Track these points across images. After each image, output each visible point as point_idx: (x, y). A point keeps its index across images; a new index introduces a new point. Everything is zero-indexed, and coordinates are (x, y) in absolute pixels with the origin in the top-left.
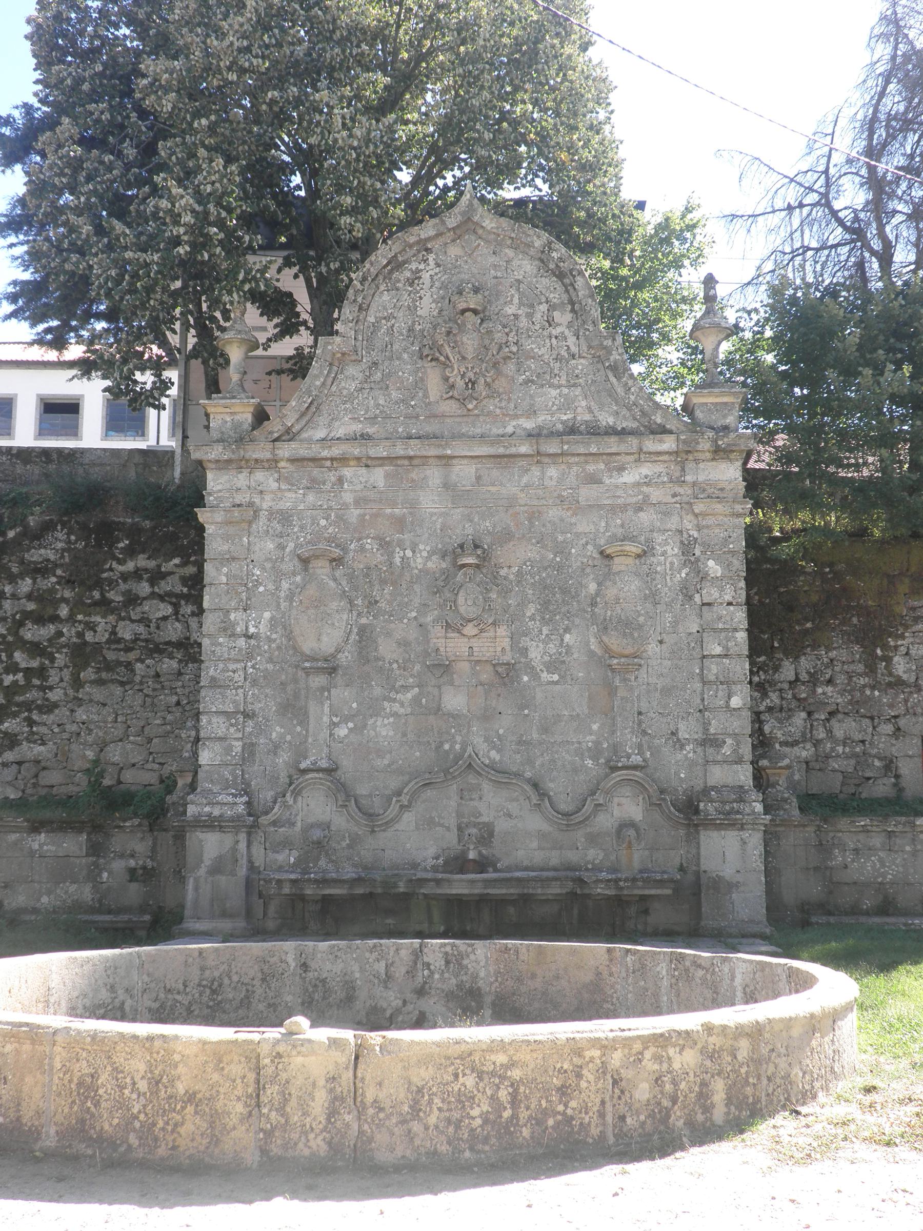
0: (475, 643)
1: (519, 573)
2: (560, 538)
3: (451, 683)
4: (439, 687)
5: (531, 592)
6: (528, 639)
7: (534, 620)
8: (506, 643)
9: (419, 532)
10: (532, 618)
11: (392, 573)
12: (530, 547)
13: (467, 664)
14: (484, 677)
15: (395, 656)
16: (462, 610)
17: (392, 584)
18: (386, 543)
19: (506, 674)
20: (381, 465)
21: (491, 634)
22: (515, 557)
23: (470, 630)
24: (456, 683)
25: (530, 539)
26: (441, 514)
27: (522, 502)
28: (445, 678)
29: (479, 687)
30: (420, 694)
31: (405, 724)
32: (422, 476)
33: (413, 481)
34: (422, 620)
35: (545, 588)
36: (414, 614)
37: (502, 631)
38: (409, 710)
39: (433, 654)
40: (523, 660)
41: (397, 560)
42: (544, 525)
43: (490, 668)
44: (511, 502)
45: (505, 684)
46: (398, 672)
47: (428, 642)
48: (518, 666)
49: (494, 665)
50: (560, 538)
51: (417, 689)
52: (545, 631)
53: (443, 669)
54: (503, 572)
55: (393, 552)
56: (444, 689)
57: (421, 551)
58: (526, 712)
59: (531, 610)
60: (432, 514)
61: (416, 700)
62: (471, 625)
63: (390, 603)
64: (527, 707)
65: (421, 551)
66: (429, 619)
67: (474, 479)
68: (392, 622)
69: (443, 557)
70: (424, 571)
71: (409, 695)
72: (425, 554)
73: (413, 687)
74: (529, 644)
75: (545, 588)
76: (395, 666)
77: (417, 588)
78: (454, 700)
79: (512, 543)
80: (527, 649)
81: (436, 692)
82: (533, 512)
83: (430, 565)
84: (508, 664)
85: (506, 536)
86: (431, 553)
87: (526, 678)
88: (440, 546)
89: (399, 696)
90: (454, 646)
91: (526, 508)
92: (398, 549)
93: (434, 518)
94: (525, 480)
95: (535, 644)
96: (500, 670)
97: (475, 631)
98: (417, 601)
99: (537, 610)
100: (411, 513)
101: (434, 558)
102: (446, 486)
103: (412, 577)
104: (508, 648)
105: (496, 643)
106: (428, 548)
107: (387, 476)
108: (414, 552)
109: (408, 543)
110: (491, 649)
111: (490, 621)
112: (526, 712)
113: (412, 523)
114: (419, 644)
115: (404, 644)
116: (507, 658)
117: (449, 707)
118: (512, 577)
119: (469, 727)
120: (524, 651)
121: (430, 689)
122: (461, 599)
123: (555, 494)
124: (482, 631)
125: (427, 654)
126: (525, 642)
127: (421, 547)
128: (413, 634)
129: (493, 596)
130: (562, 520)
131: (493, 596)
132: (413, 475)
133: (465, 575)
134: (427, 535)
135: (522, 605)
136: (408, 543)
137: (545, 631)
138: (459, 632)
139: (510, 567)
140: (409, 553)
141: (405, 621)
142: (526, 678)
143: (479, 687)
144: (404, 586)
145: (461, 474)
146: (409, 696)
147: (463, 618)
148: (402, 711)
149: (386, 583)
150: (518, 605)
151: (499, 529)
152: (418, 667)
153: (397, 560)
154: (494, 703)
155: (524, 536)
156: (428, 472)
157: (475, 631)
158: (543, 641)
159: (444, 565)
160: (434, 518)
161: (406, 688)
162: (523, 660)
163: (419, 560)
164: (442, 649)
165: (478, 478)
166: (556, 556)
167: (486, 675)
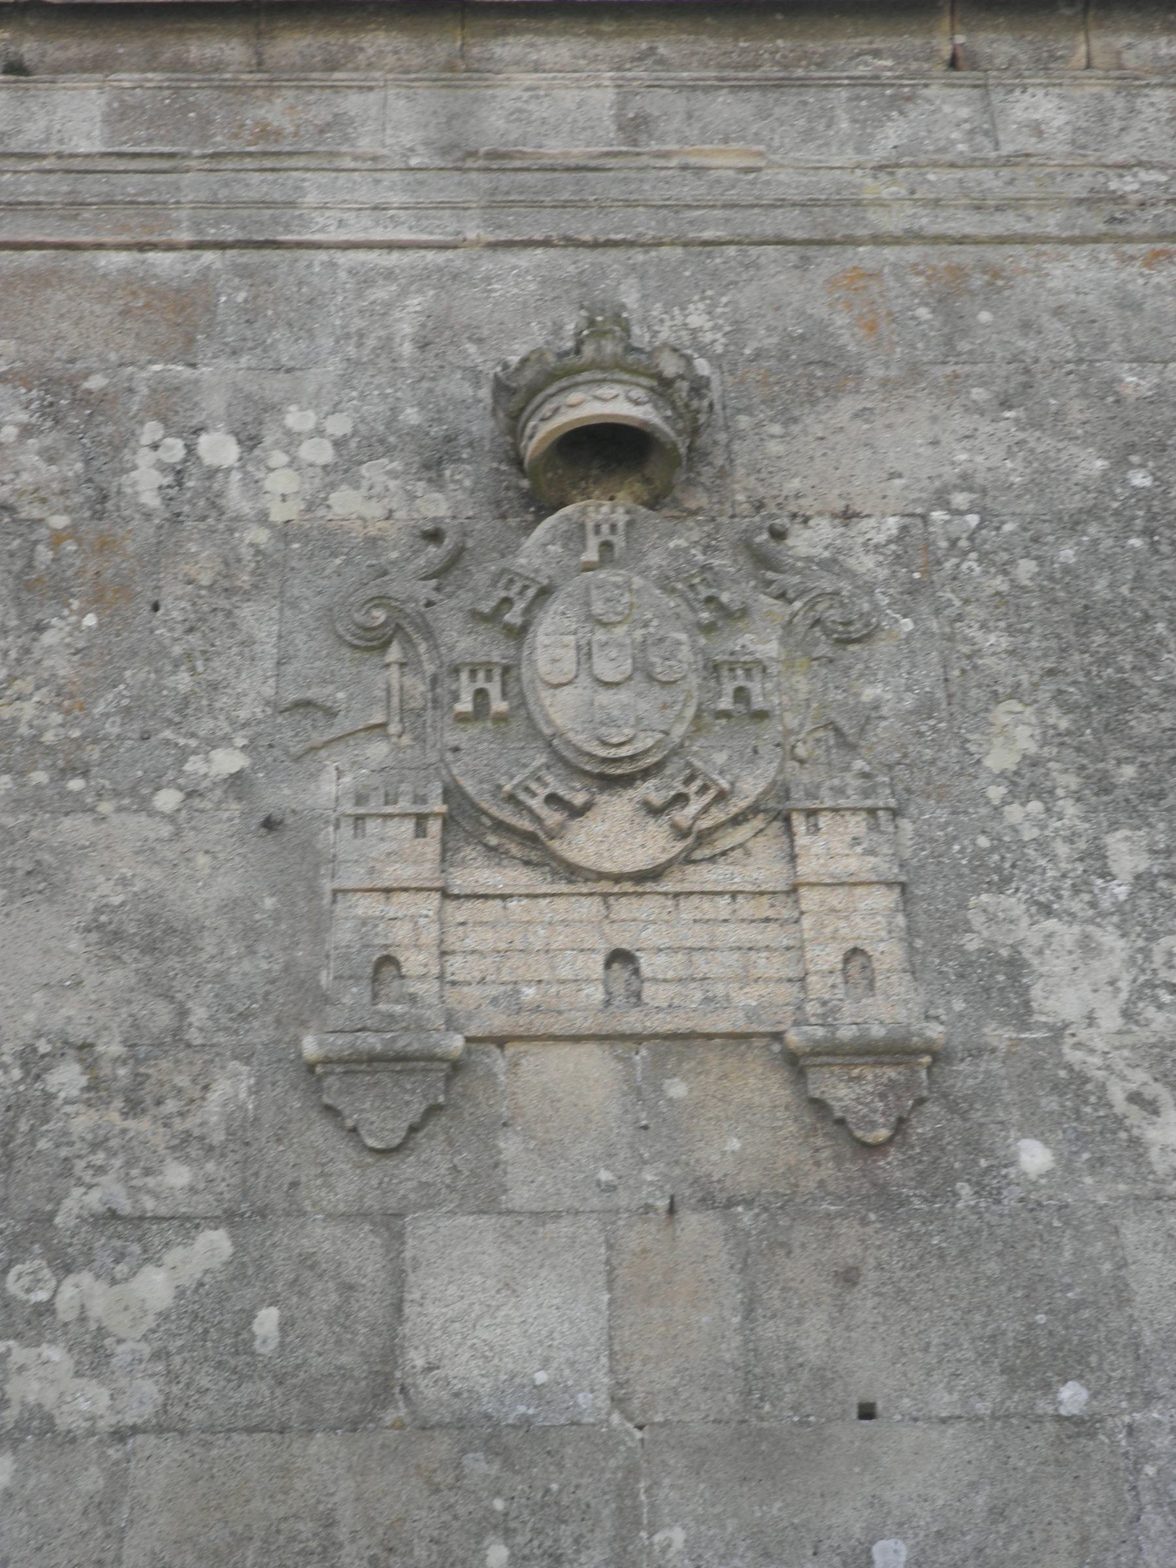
0: (643, 923)
1: (912, 547)
2: (1134, 382)
3: (484, 1195)
4: (390, 1224)
5: (996, 640)
6: (1012, 903)
7: (1047, 795)
8: (872, 918)
9: (287, 350)
10: (1027, 782)
11: (105, 546)
12: (961, 423)
13: (589, 1075)
14: (726, 1151)
15: (71, 1015)
16: (562, 710)
17: (97, 600)
18: (84, 400)
19: (885, 1116)
20: (98, 65)
21: (761, 866)
22: (861, 473)
23: (614, 834)
24: (520, 1196)
25: (955, 386)
26: (423, 277)
27: (891, 222)
28: (433, 1161)
29: (692, 1222)
30: (239, 1271)
31: (103, 1507)
32: (322, 115)
33: (265, 132)
34: (277, 797)
35: (1084, 619)
36: (228, 761)
37: (831, 848)
38: (144, 1396)
39: (355, 994)
40: (998, 1035)
41: (145, 482)
42: (1026, 326)
43: (762, 1087)
44: (824, 232)
45: (886, 1200)
46: (82, 1123)
47: (320, 925)
48: (964, 1076)
49: (796, 1064)
50: (1134, 382)
51: (215, 1244)
52: (1127, 854)
53: (416, 1089)
54: (805, 543)
55: (123, 443)
56: (426, 1235)
57: (292, 440)
58: (1072, 1396)
59: (1013, 737)
60: (365, 280)
61: (207, 1323)
62: (618, 808)
63: (66, 697)
64: (1073, 1361)
65: (292, 440)
66: (330, 787)
67: (608, 128)
68: (78, 806)
69: (434, 464)
70: (311, 538)
71: (155, 1286)
72: (319, 452)
73: (188, 1224)
74: (1029, 933)
75: (1084, 619)
76: (67, 1078)
77: (259, 621)
78: (504, 1318)
79: (848, 405)
80: (1015, 965)
81: (363, 1255)
82: (958, 272)
83: (346, 503)
84: (895, 1051)
85: (813, 373)
86: (349, 459)
87: (1034, 1157)
88: (411, 416)
89: (76, 1292)
90: (510, 949)
91: (913, 253)
92: (151, 431)
93: (381, 293)
94: (891, 136)
95: (1068, 934)
96: (841, 1092)
97: (651, 845)
98: (252, 691)
99: (1048, 736)
100: (244, 272)
101: (372, 472)
102: (459, 155)
103: (230, 563)
104: (888, 954)
105: (799, 930)
106: (339, 425)
107: (120, 115)
108: (249, 442)
109: (215, 403)
110: (763, 964)
111: (751, 787)
112: (1072, 1396)
113: (250, 314)
114: (251, 935)
115: (147, 937)
116: (889, 1009)
117: (464, 1369)
118: (864, 563)
119: (629, 1520)
120: (1004, 981)
121: (320, 1237)
122: (552, 643)
123: (1076, 187)
124: (696, 844)
125: (308, 999)
126: (999, 918)
127: (296, 418)
128: (213, 878)
129: (762, 643)
130: (1128, 304)
131: (762, 643)
132: (276, 112)
133: (576, 535)
134: (334, 366)
135: (957, 702)
136: (215, 403)
137: (1127, 854)
138: (536, 849)
139: (847, 516)
140: (218, 448)
141: (167, 799)
142: (1034, 1157)
143: (692, 1222)
144: (176, 609)
145: (538, 110)
146: (155, 1286)
147: (565, 762)
148: (88, 1402)
149: (60, 593)
150: (927, 708)
151: (762, 338)
152: (232, 1087)
153: (145, 482)
154: (814, 1336)
155: (915, 371)
156: (352, 103)
157: (651, 845)
158: (1124, 915)
159: (436, 506)
160: (381, 293)
161: (130, 1232)
162: (998, 1035)
163: (281, 481)
164: (413, 962)
165: (635, 127)
166: (1121, 462)
167: (742, 1129)
